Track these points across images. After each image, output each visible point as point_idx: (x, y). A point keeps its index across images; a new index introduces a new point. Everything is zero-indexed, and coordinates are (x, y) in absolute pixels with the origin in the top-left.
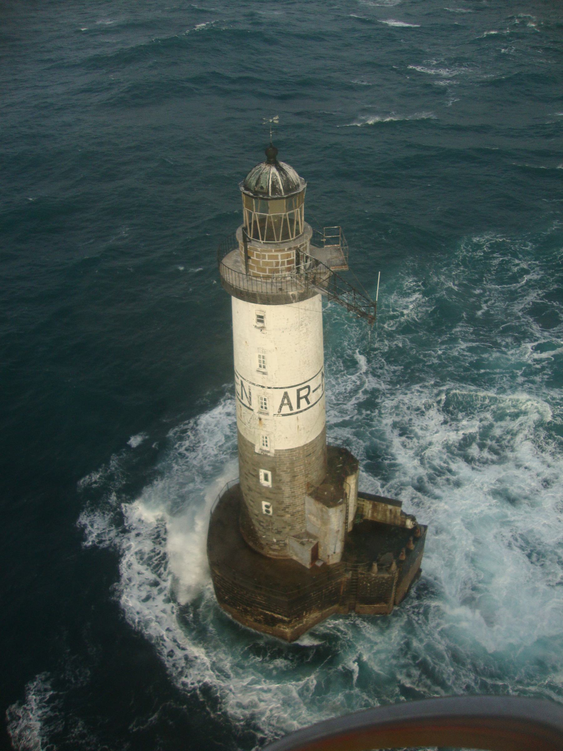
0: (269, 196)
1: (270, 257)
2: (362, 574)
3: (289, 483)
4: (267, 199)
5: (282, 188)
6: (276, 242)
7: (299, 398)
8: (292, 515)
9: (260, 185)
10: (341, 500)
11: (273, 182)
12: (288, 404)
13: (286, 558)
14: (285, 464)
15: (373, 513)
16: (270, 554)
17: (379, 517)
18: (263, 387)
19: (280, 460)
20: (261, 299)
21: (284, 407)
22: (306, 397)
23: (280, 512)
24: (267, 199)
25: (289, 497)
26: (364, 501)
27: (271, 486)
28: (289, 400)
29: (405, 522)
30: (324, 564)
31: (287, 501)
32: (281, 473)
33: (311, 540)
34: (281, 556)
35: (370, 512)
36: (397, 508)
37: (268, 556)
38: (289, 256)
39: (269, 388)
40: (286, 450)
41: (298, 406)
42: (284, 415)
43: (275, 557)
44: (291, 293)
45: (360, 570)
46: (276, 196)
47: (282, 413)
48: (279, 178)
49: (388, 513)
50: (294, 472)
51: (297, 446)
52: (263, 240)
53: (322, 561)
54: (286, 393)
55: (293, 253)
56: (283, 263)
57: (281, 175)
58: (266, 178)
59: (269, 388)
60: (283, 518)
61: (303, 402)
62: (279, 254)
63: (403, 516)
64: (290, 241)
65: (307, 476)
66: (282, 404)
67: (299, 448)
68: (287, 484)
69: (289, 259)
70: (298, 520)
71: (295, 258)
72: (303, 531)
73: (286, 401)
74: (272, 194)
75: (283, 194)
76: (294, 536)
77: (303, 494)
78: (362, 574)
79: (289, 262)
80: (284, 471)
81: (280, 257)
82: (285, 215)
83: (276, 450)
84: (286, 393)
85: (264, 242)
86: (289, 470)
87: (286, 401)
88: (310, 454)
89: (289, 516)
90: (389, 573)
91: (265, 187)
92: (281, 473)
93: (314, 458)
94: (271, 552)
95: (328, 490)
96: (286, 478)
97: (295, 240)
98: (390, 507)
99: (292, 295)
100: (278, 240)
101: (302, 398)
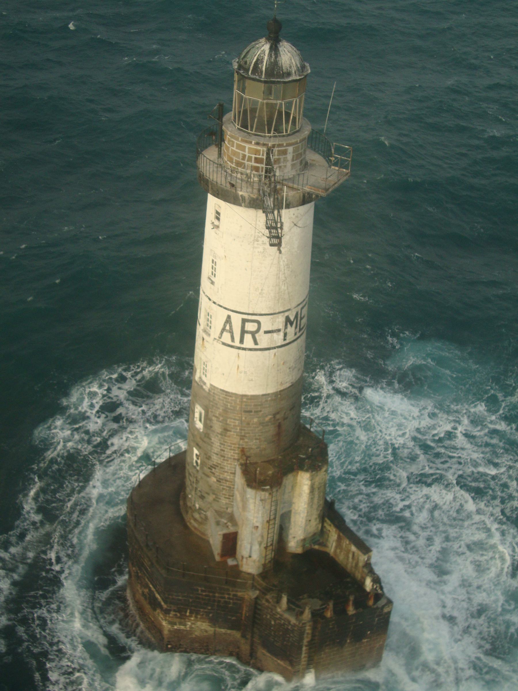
0: (261, 78)
1: (239, 147)
2: (267, 601)
3: (220, 436)
4: (246, 78)
5: (264, 69)
6: (249, 131)
7: (243, 332)
8: (217, 481)
9: (246, 59)
10: (268, 487)
11: (258, 60)
12: (230, 332)
13: (204, 537)
14: (219, 408)
15: (336, 547)
16: (191, 523)
17: (341, 558)
18: (210, 299)
19: (214, 400)
20: (212, 189)
21: (225, 333)
22: (253, 334)
23: (207, 471)
24: (246, 78)
25: (217, 454)
26: (330, 525)
27: (201, 431)
28: (231, 327)
29: (364, 579)
30: (237, 566)
31: (215, 459)
32: (214, 418)
33: (229, 524)
34: (200, 531)
35: (334, 544)
36: (360, 553)
37: (188, 524)
38: (257, 152)
39: (214, 303)
40: (221, 390)
41: (242, 341)
42: (224, 344)
43: (193, 529)
44: (240, 193)
45: (268, 597)
46: (254, 77)
47: (222, 340)
48: (266, 58)
49: (351, 556)
50: (227, 424)
51: (234, 392)
52: (238, 125)
53: (237, 561)
54: (229, 317)
55: (263, 151)
56: (250, 159)
57: (270, 55)
58: (254, 53)
59: (214, 303)
60: (208, 479)
61: (248, 338)
62: (247, 146)
63: (366, 571)
64: (265, 137)
65: (242, 437)
66: (224, 330)
67: (236, 395)
68: (217, 436)
69: (257, 156)
70: (224, 492)
71: (265, 157)
72: (229, 510)
73: (228, 328)
74: (252, 73)
75: (263, 77)
76: (216, 511)
77: (234, 459)
78: (267, 601)
79: (257, 160)
80: (216, 417)
81: (247, 150)
82: (262, 104)
83: (211, 385)
84: (229, 317)
85: (239, 127)
86: (221, 418)
87: (228, 328)
88: (251, 412)
89: (215, 480)
90: (297, 619)
91: (248, 63)
92: (214, 418)
93: (256, 420)
94: (192, 521)
95: (267, 473)
96: (217, 427)
97: (270, 137)
98: (353, 548)
99: (242, 196)
100: (252, 130)
101: (247, 332)
